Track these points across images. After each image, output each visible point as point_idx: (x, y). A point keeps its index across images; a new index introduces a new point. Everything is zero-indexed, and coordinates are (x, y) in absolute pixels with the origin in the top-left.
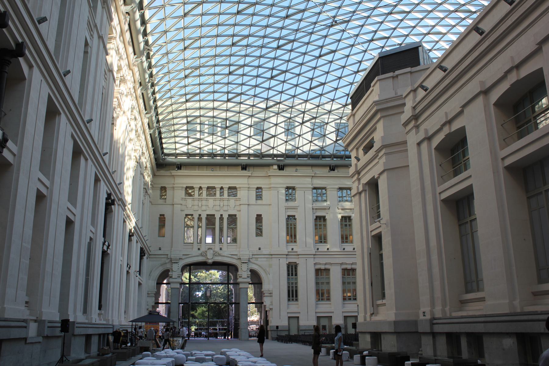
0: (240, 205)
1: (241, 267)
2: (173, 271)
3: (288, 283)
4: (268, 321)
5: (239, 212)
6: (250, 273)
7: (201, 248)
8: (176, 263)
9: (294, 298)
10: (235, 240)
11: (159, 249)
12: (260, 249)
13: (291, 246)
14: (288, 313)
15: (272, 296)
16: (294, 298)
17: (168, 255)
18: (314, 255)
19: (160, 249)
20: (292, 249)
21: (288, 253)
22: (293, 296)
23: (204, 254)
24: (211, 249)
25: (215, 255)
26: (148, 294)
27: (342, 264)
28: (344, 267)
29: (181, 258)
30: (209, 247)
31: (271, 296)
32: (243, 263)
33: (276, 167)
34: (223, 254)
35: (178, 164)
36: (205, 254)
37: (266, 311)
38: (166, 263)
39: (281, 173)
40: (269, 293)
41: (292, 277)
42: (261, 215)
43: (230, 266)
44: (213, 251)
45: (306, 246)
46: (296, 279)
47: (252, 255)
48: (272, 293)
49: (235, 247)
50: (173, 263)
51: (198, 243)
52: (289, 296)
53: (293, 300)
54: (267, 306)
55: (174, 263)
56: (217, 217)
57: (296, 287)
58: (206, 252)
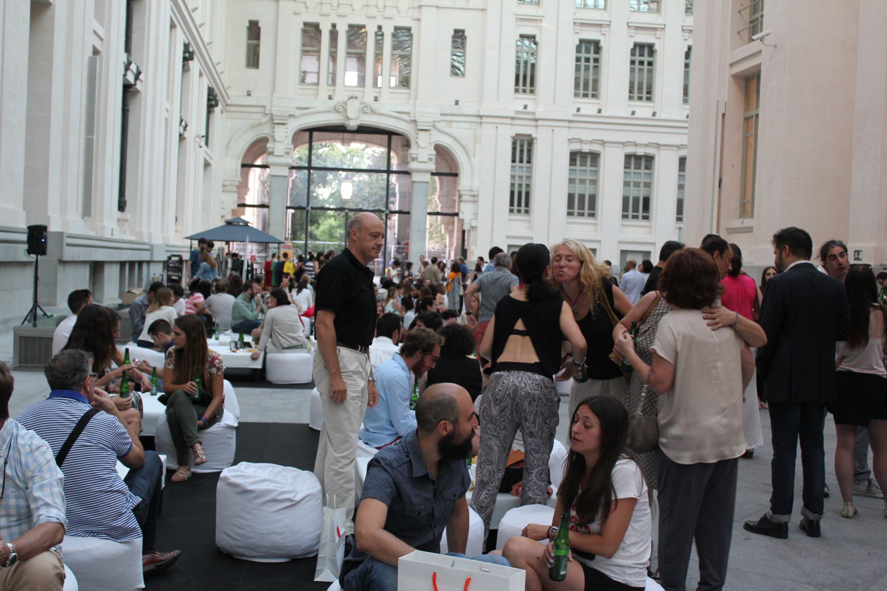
0: (420, 7)
1: (417, 138)
2: (274, 141)
3: (513, 177)
4: (466, 251)
5: (416, 22)
6: (434, 152)
7: (334, 95)
8: (283, 124)
9: (523, 208)
10: (405, 82)
11: (246, 93)
12: (457, 103)
13: (525, 99)
15: (477, 202)
16: (523, 208)
17: (264, 107)
18: (570, 121)
19: (249, 95)
20: (525, 107)
21: (516, 114)
22: (519, 205)
23: (340, 107)
24: (356, 98)
25: (364, 112)
26: (224, 186)
27: (624, 144)
28: (630, 150)
29: (293, 113)
30: (351, 94)
31: (474, 202)
32: (422, 130)
34: (381, 111)
36: (343, 107)
37: (464, 232)
38: (261, 124)
40: (472, 196)
41: (521, 165)
42: (463, 31)
43: (393, 137)
44: (362, 103)
45: (554, 102)
46: (530, 169)
47: (442, 115)
48: (478, 196)
49: (406, 96)
50: (275, 124)
51: (328, 85)
52: (512, 204)
53: (519, 211)
54: (466, 221)
55: (278, 124)
56: (371, 30)
57: (528, 186)
58: (346, 103)
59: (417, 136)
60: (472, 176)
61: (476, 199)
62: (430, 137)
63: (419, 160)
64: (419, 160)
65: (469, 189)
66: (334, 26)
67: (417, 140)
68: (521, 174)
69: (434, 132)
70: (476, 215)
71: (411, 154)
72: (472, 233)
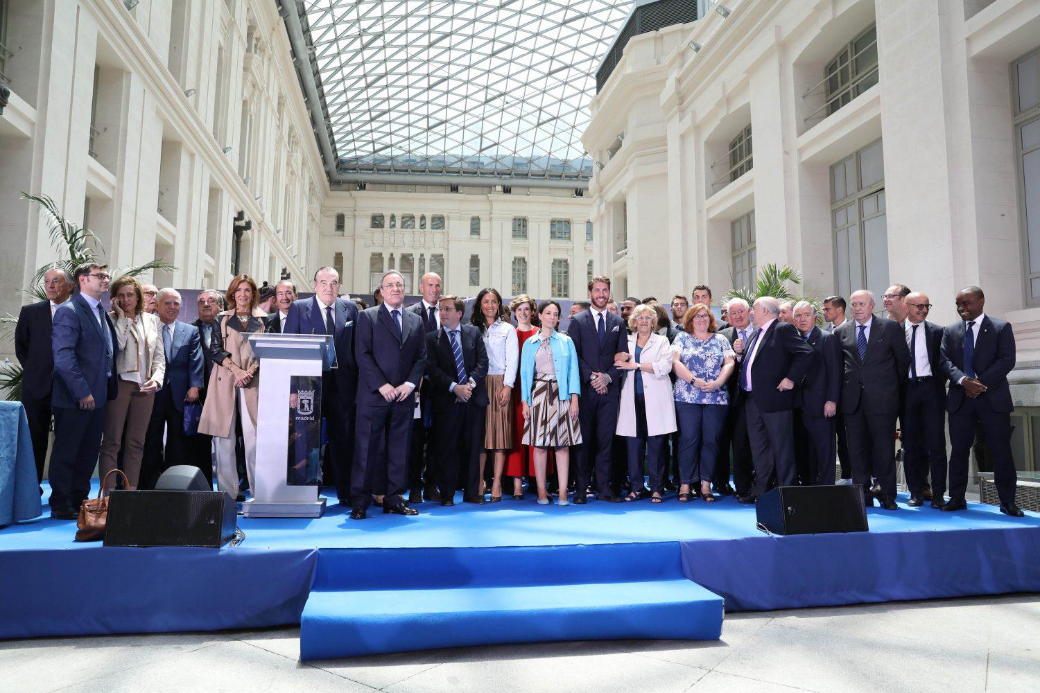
33: (499, 188)
35: (361, 182)
39: (507, 196)
42: (477, 256)
66: (392, 255)
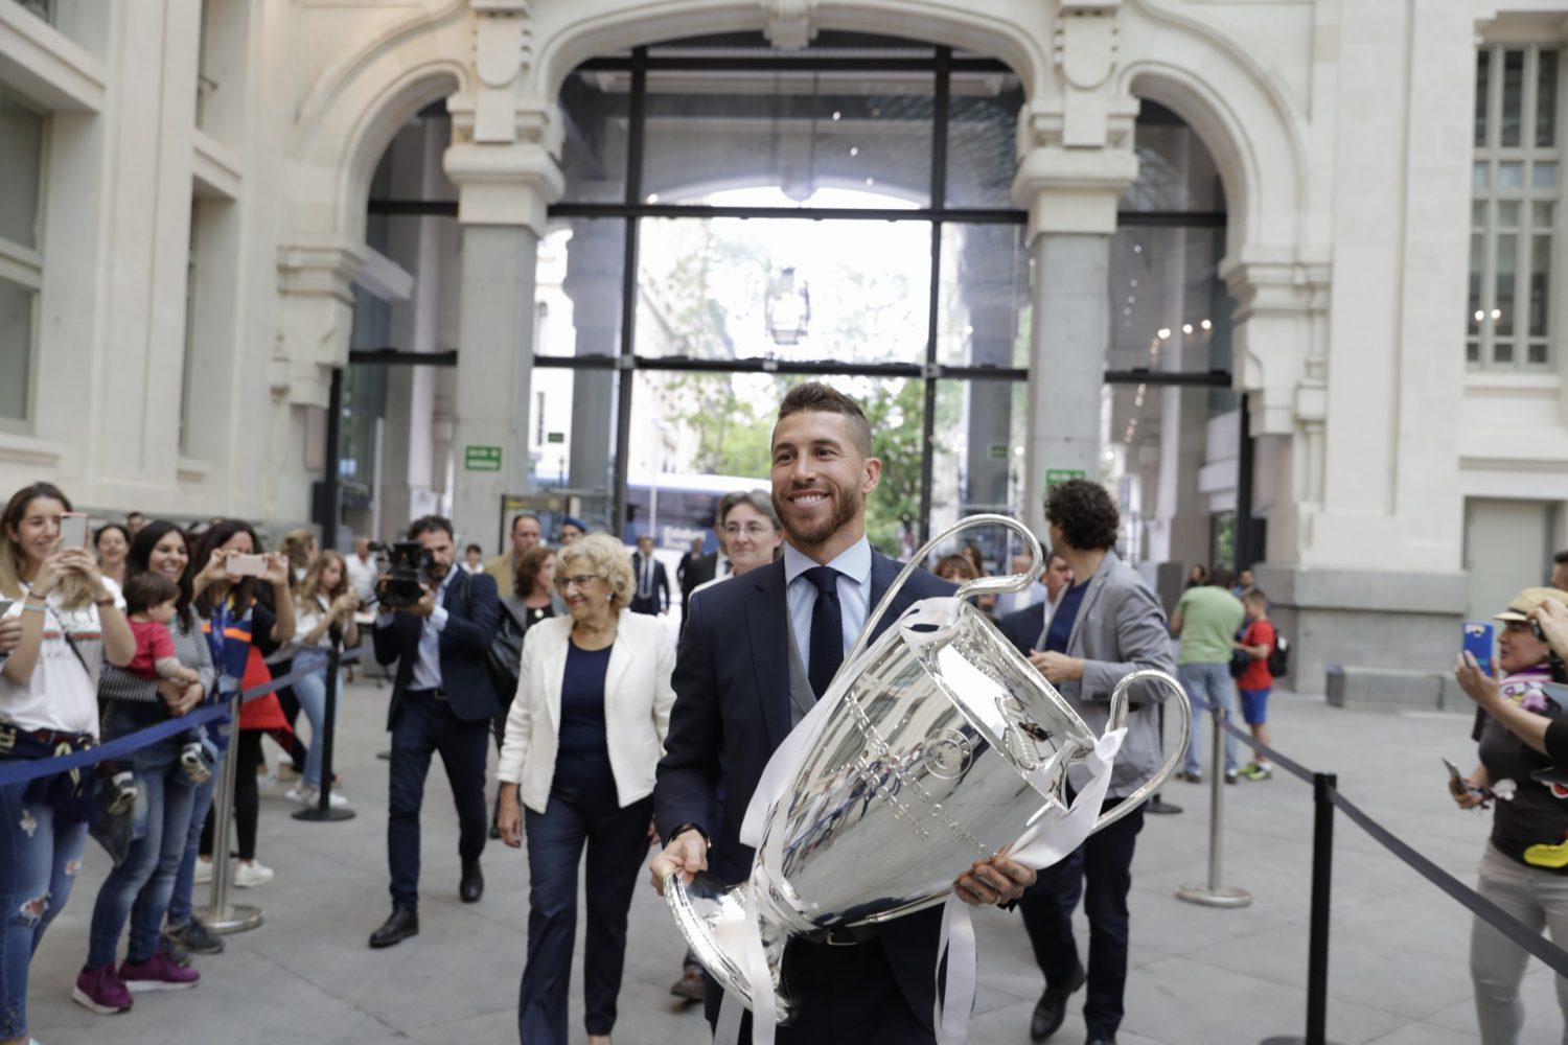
1: (1060, 49)
4: (1261, 526)
14: (1469, 463)
15: (1325, 312)
26: (284, 270)
31: (1310, 313)
40: (1298, 288)
48: (1327, 287)
54: (1270, 399)
59: (1059, 41)
60: (1300, 203)
61: (1318, 300)
62: (1114, 40)
63: (1069, 138)
64: (1069, 139)
65: (1287, 259)
67: (1058, 57)
68: (1513, 193)
69: (1130, 23)
70: (1317, 369)
71: (1033, 119)
72: (1298, 448)
